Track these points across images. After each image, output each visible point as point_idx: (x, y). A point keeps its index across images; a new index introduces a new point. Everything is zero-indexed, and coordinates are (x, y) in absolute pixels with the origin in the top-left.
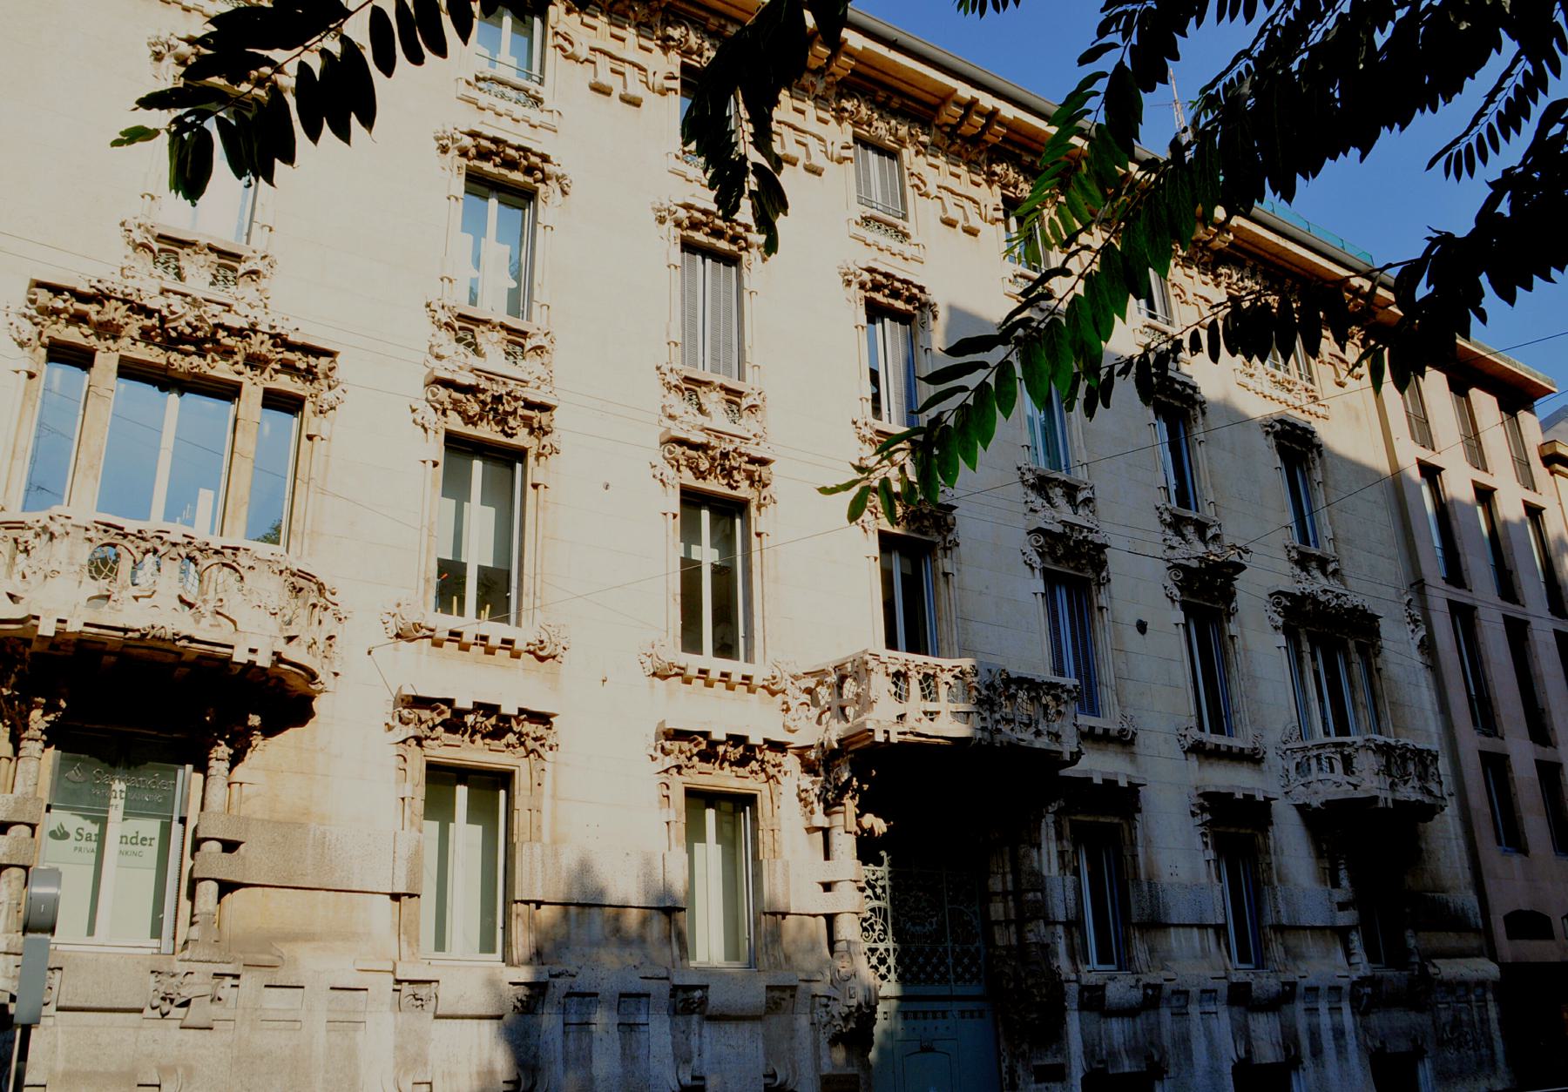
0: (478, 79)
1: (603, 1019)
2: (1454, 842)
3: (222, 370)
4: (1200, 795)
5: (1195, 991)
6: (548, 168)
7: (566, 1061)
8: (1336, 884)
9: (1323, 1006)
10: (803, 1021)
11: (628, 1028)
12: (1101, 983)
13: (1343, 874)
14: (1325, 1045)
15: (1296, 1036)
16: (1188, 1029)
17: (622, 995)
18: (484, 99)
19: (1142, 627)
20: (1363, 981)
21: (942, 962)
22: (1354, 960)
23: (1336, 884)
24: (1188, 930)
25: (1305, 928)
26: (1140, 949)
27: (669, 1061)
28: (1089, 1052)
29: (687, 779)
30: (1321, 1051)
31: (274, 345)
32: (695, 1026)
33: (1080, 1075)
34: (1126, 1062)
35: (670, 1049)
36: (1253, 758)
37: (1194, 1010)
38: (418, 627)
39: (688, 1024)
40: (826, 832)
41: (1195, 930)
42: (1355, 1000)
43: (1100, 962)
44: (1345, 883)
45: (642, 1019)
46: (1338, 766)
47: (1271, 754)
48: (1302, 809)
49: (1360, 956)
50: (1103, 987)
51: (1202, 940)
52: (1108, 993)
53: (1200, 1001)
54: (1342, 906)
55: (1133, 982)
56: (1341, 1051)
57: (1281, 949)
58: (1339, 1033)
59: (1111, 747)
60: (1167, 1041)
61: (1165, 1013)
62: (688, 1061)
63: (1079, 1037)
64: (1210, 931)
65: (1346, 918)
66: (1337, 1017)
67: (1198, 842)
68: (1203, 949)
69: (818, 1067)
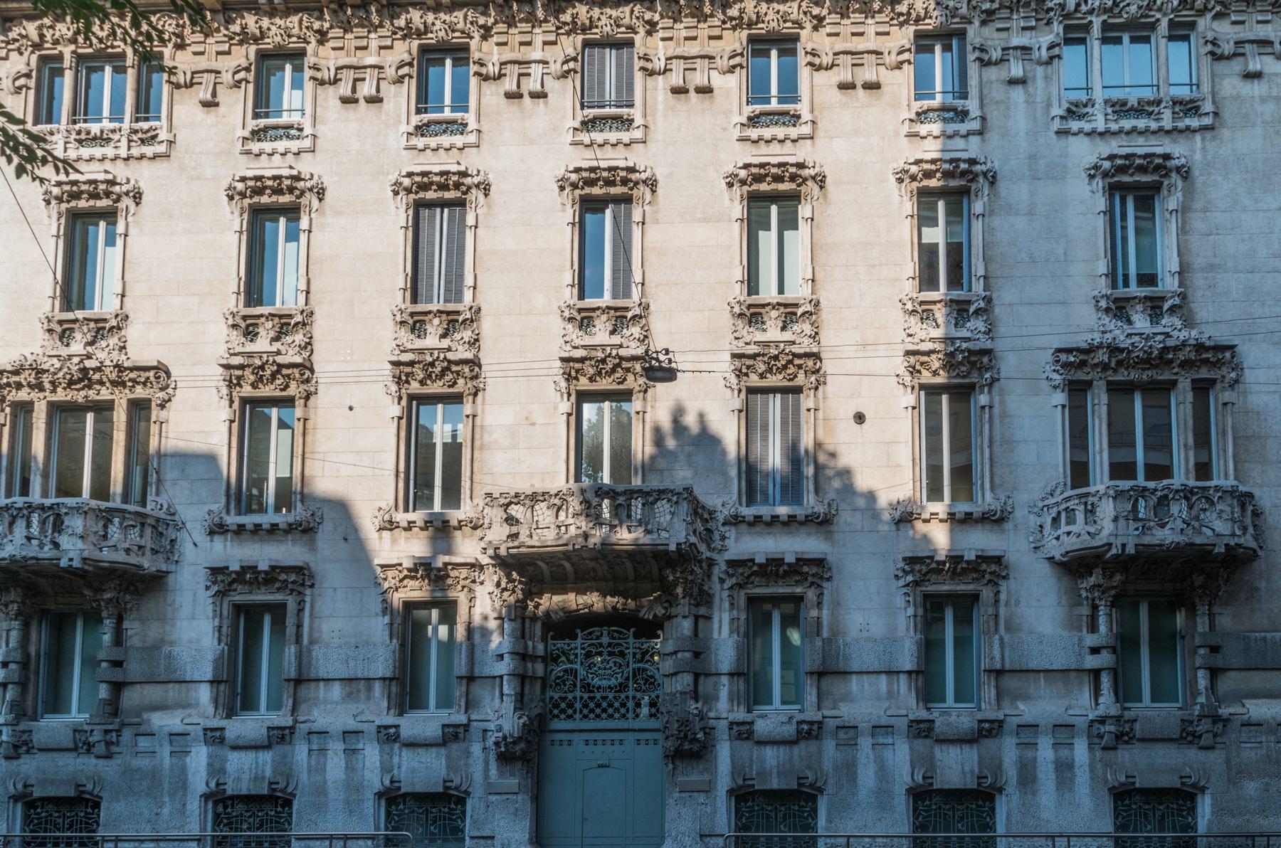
1: (336, 747)
3: (105, 394)
4: (905, 559)
5: (863, 726)
7: (309, 771)
8: (1093, 628)
10: (476, 749)
11: (351, 752)
13: (1102, 620)
14: (1041, 775)
15: (1000, 767)
16: (854, 758)
19: (860, 418)
20: (1102, 720)
21: (623, 705)
24: (873, 677)
27: (378, 771)
28: (735, 770)
29: (402, 595)
32: (396, 750)
33: (726, 789)
35: (378, 764)
36: (995, 520)
37: (865, 743)
39: (392, 749)
41: (883, 678)
42: (1094, 737)
45: (360, 746)
46: (1080, 516)
47: (1020, 514)
49: (1107, 697)
51: (890, 684)
53: (873, 736)
54: (1095, 651)
55: (785, 719)
57: (993, 691)
58: (1064, 769)
59: (804, 529)
60: (827, 764)
61: (829, 746)
62: (391, 771)
63: (728, 761)
64: (903, 678)
65: (1091, 662)
66: (1064, 753)
67: (900, 601)
69: (486, 777)
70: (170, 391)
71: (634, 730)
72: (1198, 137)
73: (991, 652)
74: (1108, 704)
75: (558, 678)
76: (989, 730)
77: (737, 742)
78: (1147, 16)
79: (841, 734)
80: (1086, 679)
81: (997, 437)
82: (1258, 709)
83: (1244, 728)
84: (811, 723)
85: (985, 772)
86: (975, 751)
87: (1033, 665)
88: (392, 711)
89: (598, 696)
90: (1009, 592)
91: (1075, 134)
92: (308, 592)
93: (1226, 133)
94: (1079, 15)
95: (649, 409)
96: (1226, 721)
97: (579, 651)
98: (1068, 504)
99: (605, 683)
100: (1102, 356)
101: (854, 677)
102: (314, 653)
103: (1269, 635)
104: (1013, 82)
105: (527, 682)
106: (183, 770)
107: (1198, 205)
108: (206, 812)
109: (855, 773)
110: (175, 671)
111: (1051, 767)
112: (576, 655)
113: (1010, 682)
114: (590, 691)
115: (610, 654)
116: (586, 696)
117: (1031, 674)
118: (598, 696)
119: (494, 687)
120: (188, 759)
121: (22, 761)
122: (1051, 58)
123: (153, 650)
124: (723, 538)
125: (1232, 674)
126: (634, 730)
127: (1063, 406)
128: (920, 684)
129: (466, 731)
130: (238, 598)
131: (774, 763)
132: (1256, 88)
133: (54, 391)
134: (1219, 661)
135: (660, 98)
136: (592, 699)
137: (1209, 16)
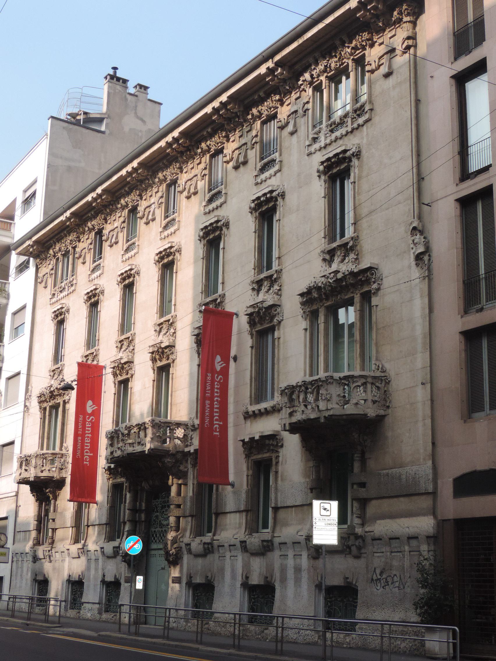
2: (420, 424)
5: (226, 545)
9: (291, 553)
25: (292, 507)
31: (58, 390)
33: (185, 582)
34: (198, 578)
37: (228, 554)
41: (238, 514)
55: (199, 542)
56: (298, 580)
58: (298, 570)
61: (216, 555)
66: (298, 561)
69: (125, 574)
70: (70, 395)
72: (365, 127)
75: (154, 520)
76: (267, 547)
77: (189, 555)
78: (343, 64)
79: (220, 548)
81: (281, 357)
82: (382, 527)
83: (375, 542)
84: (208, 544)
85: (268, 575)
86: (265, 560)
87: (288, 504)
88: (106, 541)
90: (283, 455)
91: (314, 153)
93: (376, 119)
94: (316, 79)
95: (174, 372)
96: (362, 538)
101: (229, 515)
103: (390, 471)
104: (292, 134)
105: (138, 524)
107: (364, 174)
108: (68, 588)
109: (224, 573)
111: (293, 570)
113: (281, 514)
114: (162, 528)
116: (160, 530)
117: (290, 509)
118: (163, 529)
121: (36, 563)
122: (305, 112)
123: (61, 513)
124: (191, 439)
125: (374, 502)
127: (306, 330)
128: (249, 518)
131: (200, 567)
132: (391, 80)
133: (50, 401)
134: (362, 493)
135: (184, 204)
136: (162, 531)
137: (367, 48)
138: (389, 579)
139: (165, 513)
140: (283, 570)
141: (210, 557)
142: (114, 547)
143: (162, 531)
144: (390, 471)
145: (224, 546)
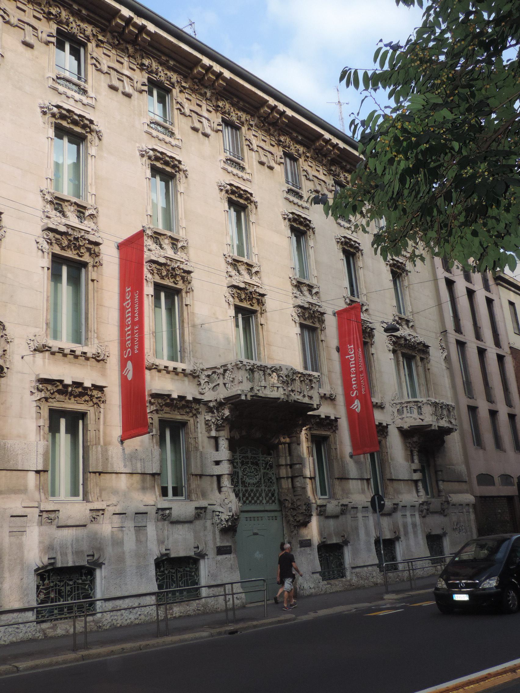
0: (58, 78)
5: (360, 507)
6: (93, 127)
8: (413, 462)
9: (408, 514)
10: (209, 523)
12: (325, 504)
17: (136, 514)
18: (61, 89)
21: (260, 495)
22: (421, 494)
23: (413, 462)
25: (401, 480)
26: (338, 490)
27: (155, 543)
29: (160, 416)
30: (408, 533)
38: (44, 346)
40: (216, 439)
41: (359, 481)
43: (322, 495)
44: (416, 461)
48: (400, 429)
49: (422, 492)
50: (325, 506)
52: (327, 509)
54: (415, 471)
56: (415, 533)
58: (414, 525)
61: (349, 516)
62: (163, 542)
64: (365, 481)
65: (417, 476)
66: (414, 519)
68: (362, 489)
69: (215, 543)
71: (267, 511)
73: (390, 471)
74: (423, 497)
80: (413, 484)
89: (249, 489)
92: (102, 405)
97: (239, 461)
98: (408, 404)
99: (252, 481)
100: (403, 342)
101: (350, 481)
102: (110, 453)
103: (450, 467)
106: (21, 547)
110: (9, 461)
112: (237, 463)
115: (252, 463)
117: (400, 482)
118: (249, 489)
119: (212, 483)
120: (24, 538)
126: (267, 511)
129: (205, 512)
130: (56, 405)
138: (461, 528)
139: (248, 469)
140: (405, 526)
141: (342, 519)
142: (197, 508)
143: (246, 491)
144: (450, 467)
145: (357, 508)
